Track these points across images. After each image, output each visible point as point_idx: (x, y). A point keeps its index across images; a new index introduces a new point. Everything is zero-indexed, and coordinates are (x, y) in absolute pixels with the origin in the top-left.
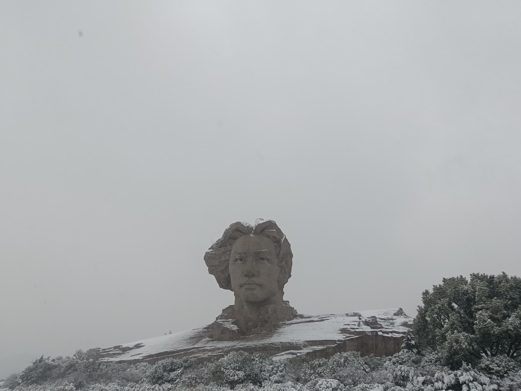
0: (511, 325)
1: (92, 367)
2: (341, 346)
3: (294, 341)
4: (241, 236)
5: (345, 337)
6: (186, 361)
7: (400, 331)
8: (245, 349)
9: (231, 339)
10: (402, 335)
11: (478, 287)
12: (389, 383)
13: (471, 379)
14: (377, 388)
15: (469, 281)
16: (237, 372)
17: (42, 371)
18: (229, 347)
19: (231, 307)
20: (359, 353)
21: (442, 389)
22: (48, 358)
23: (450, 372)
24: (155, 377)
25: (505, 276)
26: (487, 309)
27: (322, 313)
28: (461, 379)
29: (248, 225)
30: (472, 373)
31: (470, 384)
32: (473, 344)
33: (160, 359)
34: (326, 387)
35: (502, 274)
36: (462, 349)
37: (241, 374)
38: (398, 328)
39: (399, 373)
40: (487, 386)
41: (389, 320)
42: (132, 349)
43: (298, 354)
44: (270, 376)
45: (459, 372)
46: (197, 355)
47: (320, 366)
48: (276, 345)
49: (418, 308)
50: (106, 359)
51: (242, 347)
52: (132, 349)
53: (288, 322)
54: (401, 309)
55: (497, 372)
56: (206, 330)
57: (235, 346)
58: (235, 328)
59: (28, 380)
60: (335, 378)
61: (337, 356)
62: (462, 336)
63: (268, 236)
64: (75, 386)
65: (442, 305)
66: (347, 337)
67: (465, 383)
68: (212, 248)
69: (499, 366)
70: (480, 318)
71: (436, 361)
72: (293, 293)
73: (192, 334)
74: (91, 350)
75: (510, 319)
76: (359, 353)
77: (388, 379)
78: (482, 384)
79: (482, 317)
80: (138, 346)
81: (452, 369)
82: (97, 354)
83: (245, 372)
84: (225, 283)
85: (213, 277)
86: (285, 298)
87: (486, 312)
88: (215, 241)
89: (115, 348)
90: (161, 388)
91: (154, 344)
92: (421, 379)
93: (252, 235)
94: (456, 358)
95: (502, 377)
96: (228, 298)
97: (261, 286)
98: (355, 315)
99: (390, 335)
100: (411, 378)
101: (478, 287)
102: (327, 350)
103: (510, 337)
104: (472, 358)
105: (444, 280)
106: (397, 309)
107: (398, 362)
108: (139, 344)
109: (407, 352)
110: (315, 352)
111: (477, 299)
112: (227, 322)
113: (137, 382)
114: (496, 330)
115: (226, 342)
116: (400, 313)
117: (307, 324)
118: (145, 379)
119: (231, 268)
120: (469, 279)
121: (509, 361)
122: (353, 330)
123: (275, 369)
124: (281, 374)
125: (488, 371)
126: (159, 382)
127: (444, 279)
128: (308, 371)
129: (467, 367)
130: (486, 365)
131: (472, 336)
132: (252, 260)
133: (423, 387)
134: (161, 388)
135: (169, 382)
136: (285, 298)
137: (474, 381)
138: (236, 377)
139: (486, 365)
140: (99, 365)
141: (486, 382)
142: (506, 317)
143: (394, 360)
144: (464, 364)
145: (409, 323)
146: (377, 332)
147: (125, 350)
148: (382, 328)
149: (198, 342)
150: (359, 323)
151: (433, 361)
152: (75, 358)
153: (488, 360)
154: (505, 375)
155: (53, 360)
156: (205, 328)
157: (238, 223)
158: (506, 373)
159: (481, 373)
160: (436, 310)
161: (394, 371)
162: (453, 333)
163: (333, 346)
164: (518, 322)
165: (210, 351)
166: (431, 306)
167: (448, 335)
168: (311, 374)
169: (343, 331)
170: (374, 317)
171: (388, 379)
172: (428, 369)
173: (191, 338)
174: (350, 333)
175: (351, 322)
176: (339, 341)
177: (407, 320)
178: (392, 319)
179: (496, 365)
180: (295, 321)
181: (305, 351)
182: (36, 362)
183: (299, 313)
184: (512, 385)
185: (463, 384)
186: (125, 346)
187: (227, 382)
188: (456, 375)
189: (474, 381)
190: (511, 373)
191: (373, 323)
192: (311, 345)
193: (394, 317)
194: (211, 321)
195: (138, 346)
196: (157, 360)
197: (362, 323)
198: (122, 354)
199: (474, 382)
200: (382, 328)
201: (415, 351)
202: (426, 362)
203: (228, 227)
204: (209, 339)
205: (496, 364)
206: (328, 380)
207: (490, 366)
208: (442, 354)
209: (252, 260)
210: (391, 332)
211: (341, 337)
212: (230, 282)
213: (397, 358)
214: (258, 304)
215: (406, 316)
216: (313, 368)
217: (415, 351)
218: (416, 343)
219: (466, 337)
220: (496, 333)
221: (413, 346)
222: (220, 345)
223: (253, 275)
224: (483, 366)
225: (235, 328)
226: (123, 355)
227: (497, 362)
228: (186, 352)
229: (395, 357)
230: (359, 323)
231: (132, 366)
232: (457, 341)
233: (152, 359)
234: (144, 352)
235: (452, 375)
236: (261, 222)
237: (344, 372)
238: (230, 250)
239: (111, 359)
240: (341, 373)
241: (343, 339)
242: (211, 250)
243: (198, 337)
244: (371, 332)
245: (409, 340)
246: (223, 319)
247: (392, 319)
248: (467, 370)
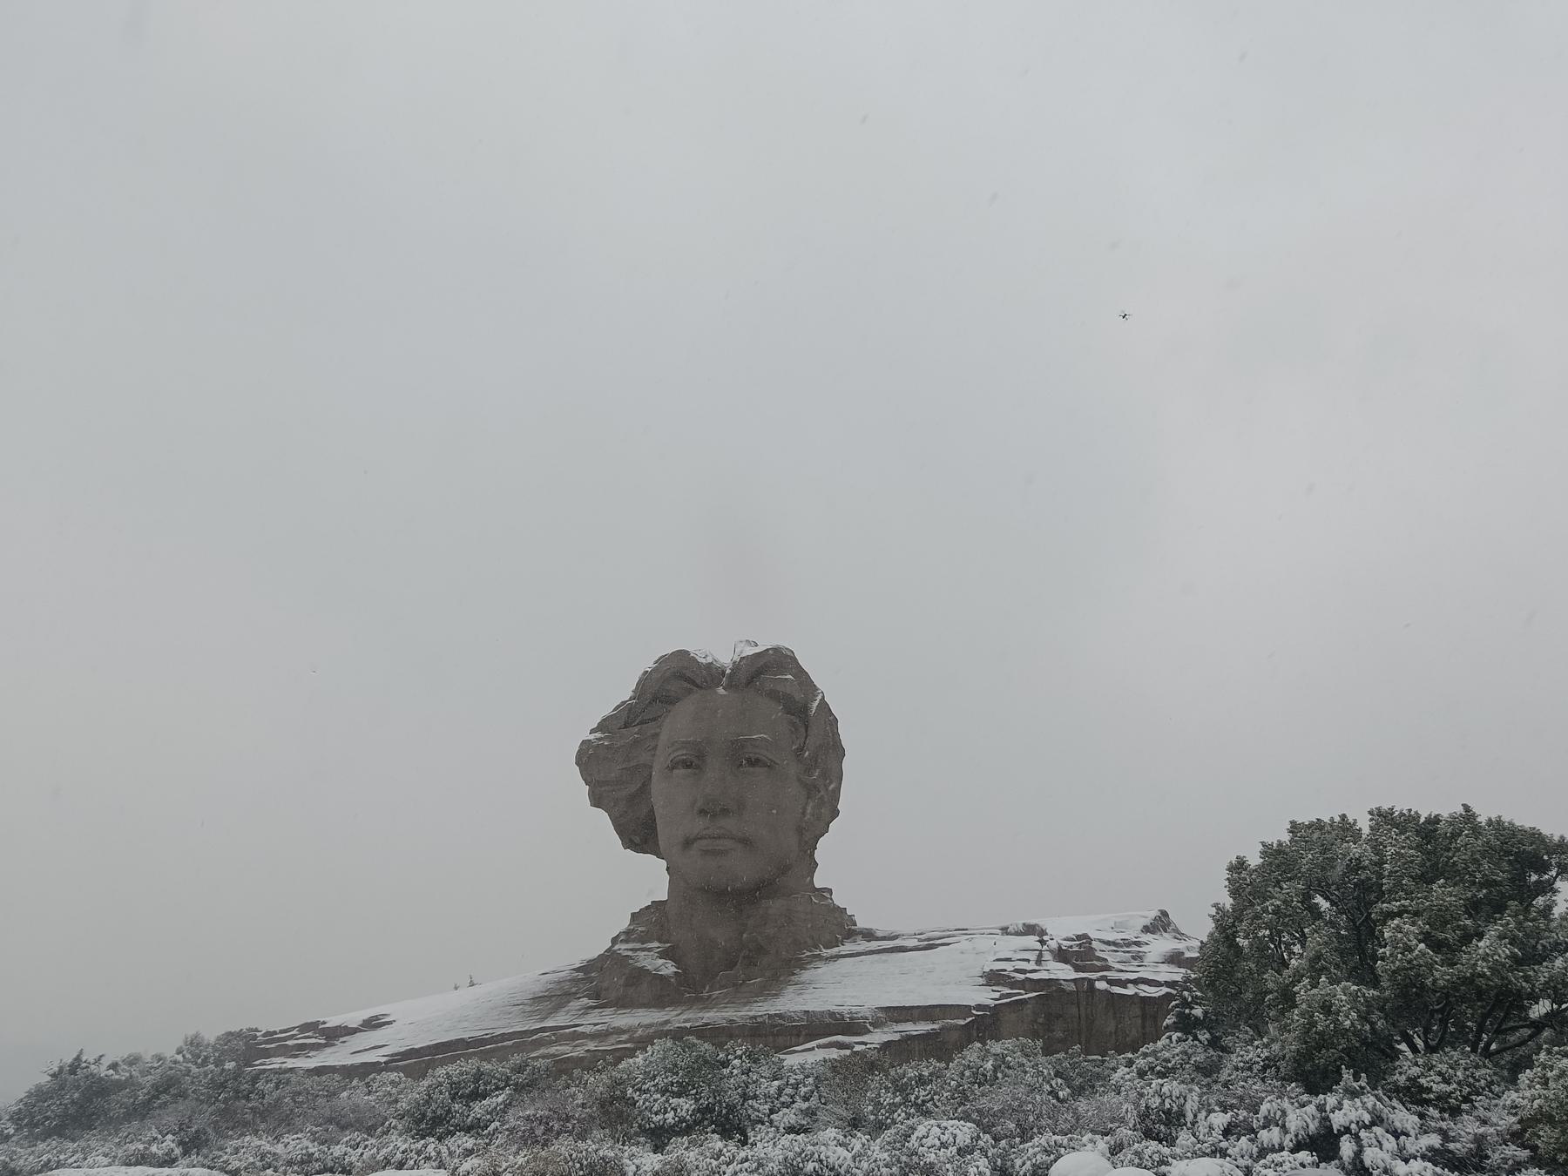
0: (1483, 959)
1: (232, 1087)
2: (985, 1024)
3: (845, 1010)
4: (690, 692)
5: (997, 995)
6: (519, 1069)
7: (1161, 978)
8: (703, 1032)
9: (659, 1003)
10: (1165, 990)
11: (1390, 850)
12: (1125, 1133)
13: (1367, 1118)
14: (1090, 1146)
15: (1366, 831)
16: (674, 1101)
17: (80, 1103)
19: (657, 905)
20: (1040, 1043)
21: (1282, 1149)
22: (98, 1061)
23: (1305, 1098)
24: (424, 1115)
25: (1469, 815)
26: (1417, 914)
27: (931, 924)
28: (1338, 1120)
29: (709, 660)
30: (1370, 1100)
31: (1363, 1134)
32: (1374, 1017)
33: (443, 1063)
34: (938, 1143)
35: (1461, 810)
36: (1341, 1032)
37: (686, 1105)
38: (1154, 969)
39: (1155, 1102)
40: (1412, 1139)
41: (1128, 945)
42: (354, 1031)
43: (858, 1048)
44: (772, 1111)
45: (1331, 1100)
46: (552, 1050)
47: (921, 1082)
48: (791, 1019)
49: (1213, 911)
50: (276, 1063)
52: (354, 1031)
53: (826, 952)
54: (1165, 914)
55: (1442, 1098)
56: (581, 975)
57: (667, 1022)
58: (669, 968)
59: (36, 1126)
60: (966, 1117)
61: (972, 1054)
62: (1342, 993)
63: (774, 695)
64: (181, 1143)
65: (1285, 902)
66: (1003, 996)
67: (1347, 1130)
68: (602, 727)
69: (1447, 1081)
70: (1395, 943)
71: (1264, 1068)
72: (844, 865)
73: (538, 989)
74: (230, 1034)
75: (1481, 944)
76: (1040, 1043)
77: (1122, 1121)
78: (1396, 1134)
79: (1401, 938)
80: (373, 1024)
81: (1313, 1090)
82: (248, 1046)
83: (697, 1100)
84: (639, 834)
85: (602, 818)
86: (819, 881)
87: (1413, 924)
88: (607, 710)
89: (305, 1028)
90: (444, 1150)
91: (421, 1018)
92: (1220, 1119)
93: (721, 690)
94: (1323, 1058)
95: (1455, 1112)
96: (648, 879)
97: (745, 842)
98: (1030, 930)
99: (1130, 990)
100: (1190, 1117)
101: (1390, 850)
102: (943, 1035)
103: (1480, 994)
104: (1371, 1058)
105: (1294, 828)
106: (1154, 913)
107: (1152, 1069)
108: (377, 1017)
109: (1179, 1040)
110: (908, 1039)
111: (1387, 884)
112: (643, 950)
113: (370, 1131)
114: (1442, 975)
115: (641, 1012)
116: (1161, 924)
117: (884, 956)
118: (394, 1122)
119: (658, 788)
120: (1364, 825)
121: (1477, 1067)
122: (1022, 976)
123: (789, 1091)
124: (806, 1105)
125: (1414, 1095)
126: (440, 1130)
127: (1293, 823)
128: (887, 1099)
129: (1355, 1085)
130: (1409, 1079)
131: (1372, 992)
132: (721, 764)
133: (1224, 1144)
134: (444, 1150)
135: (468, 1130)
136: (819, 881)
137: (1373, 1124)
138: (671, 1115)
139: (1409, 1079)
140: (255, 1079)
141: (1408, 1126)
142: (1468, 937)
143: (1141, 1063)
144: (1347, 1075)
145: (1188, 955)
146: (1091, 982)
147: (334, 1035)
148: (1108, 968)
149: (556, 1009)
150: (1040, 956)
151: (1256, 1068)
152: (180, 1057)
153: (1416, 1064)
154: (1464, 1106)
155: (114, 1066)
156: (577, 970)
157: (682, 654)
158: (1466, 1099)
159: (1395, 1103)
160: (1267, 917)
161: (1142, 1095)
162: (1314, 986)
163: (962, 1022)
164: (1505, 951)
165: (592, 1036)
166: (1253, 905)
167: (1301, 990)
168: (893, 1107)
169: (993, 978)
170: (1085, 936)
171: (1122, 1121)
172: (1240, 1092)
173: (536, 999)
174: (1013, 984)
175: (1015, 952)
176: (979, 1007)
177: (1181, 946)
178: (1138, 944)
179: (1439, 1079)
180: (848, 947)
181: (877, 1038)
182: (61, 1069)
183: (861, 923)
184: (1483, 1136)
185: (1341, 1134)
186: (333, 1021)
187: (643, 1131)
188: (1321, 1108)
189: (1373, 1124)
190: (1480, 1101)
191: (1080, 953)
193: (1145, 938)
194: (597, 947)
195: (373, 1024)
196: (432, 1065)
197: (1047, 956)
198: (325, 1045)
199: (1378, 1130)
200: (1108, 968)
201: (1204, 1036)
202: (1237, 1069)
203: (648, 664)
204: (591, 1003)
205: (1440, 1074)
206: (944, 1124)
207: (1422, 1081)
208: (1283, 1048)
209: (721, 764)
210: (1135, 982)
211: (987, 996)
212: (654, 829)
213: (1150, 1059)
214: (739, 899)
215: (1179, 935)
216: (901, 1088)
217: (1204, 1036)
218: (1206, 1013)
219: (1354, 997)
220: (1441, 982)
221: (1198, 1023)
222: (624, 1019)
223: (725, 812)
224: (1402, 1080)
225: (669, 968)
226: (329, 1050)
227: (1443, 1068)
228: (523, 1041)
229: (1145, 1055)
230: (1040, 956)
231: (355, 1082)
232: (1326, 1008)
233: (415, 1061)
234: (392, 1041)
235: (1311, 1109)
236: (750, 651)
237: (993, 1100)
238: (657, 735)
239: (290, 1063)
240: (984, 1103)
241: (992, 1003)
242: (598, 735)
243: (555, 997)
244: (1074, 981)
245: (1185, 1004)
247: (1138, 944)
248: (1353, 1094)
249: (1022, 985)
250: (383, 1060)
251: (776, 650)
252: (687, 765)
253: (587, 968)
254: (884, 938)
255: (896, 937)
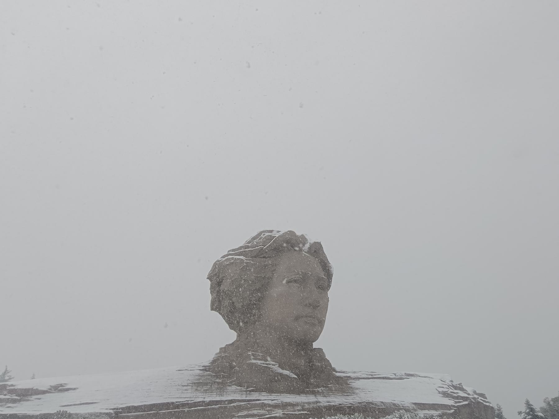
9: (290, 391)
18: (309, 403)
42: (44, 392)
46: (255, 412)
48: (376, 404)
51: (333, 404)
52: (44, 392)
80: (59, 389)
99: (485, 403)
108: (61, 385)
119: (278, 288)
145: (477, 392)
147: (25, 394)
157: (292, 233)
192: (422, 409)
198: (20, 401)
246: (260, 360)
249: (454, 398)
250: (112, 411)
251: (319, 244)
252: (295, 281)
253: (205, 369)
254: (339, 372)
255: (344, 372)
